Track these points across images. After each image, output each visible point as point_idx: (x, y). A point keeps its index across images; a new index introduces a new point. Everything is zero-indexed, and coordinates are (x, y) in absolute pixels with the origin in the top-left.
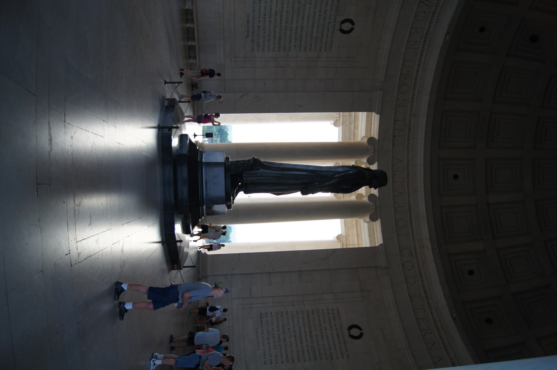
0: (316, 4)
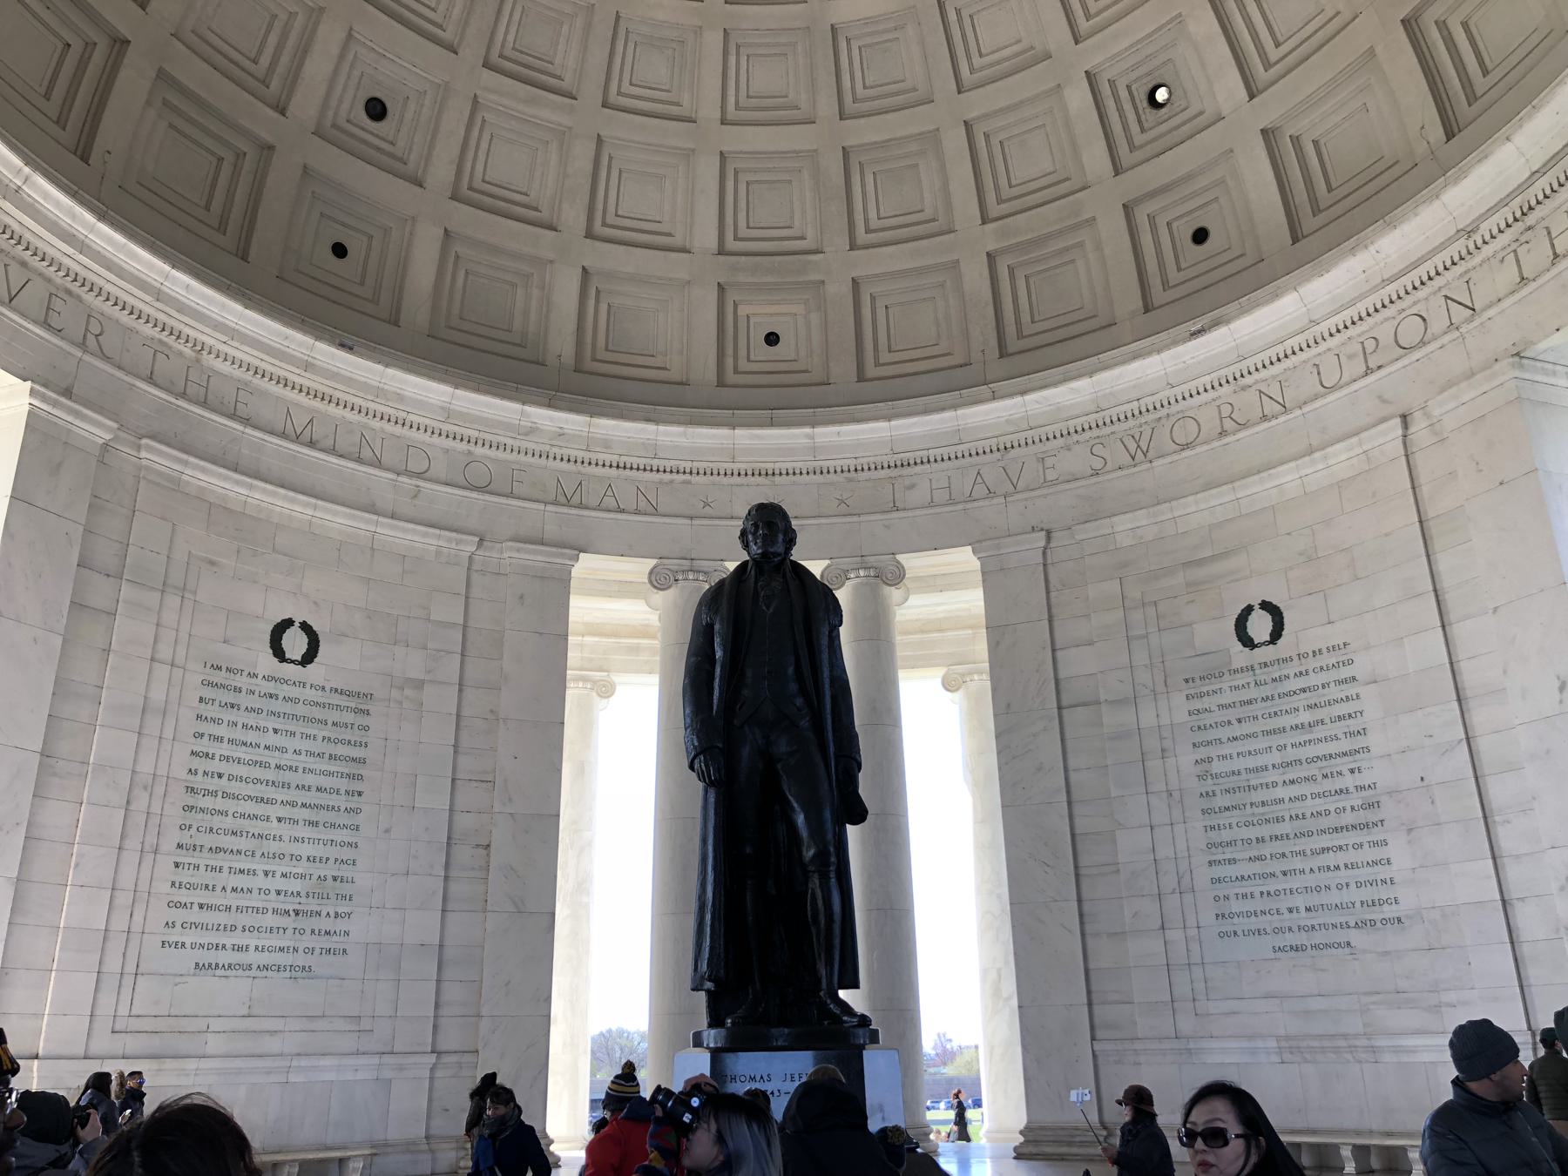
0: (1209, 743)
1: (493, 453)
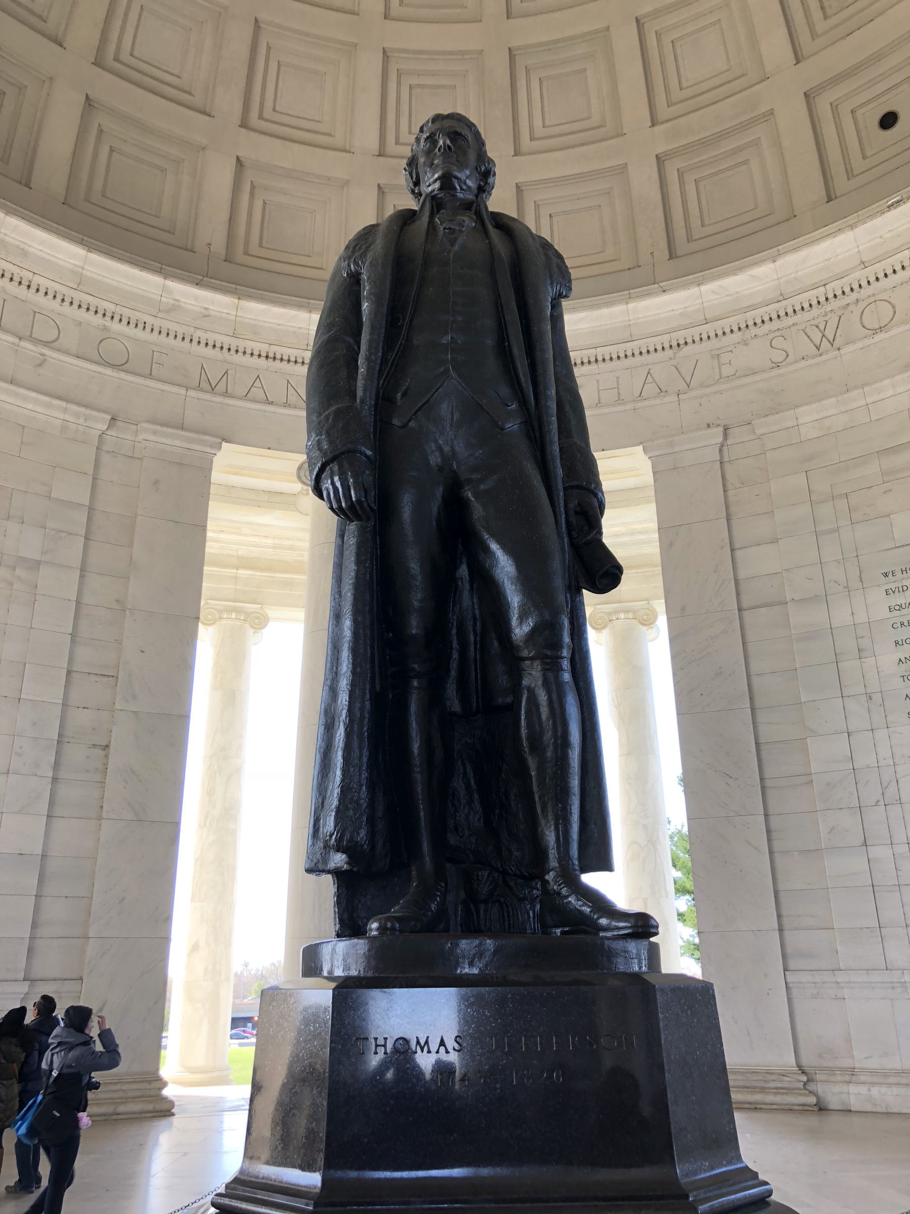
1: (131, 331)
